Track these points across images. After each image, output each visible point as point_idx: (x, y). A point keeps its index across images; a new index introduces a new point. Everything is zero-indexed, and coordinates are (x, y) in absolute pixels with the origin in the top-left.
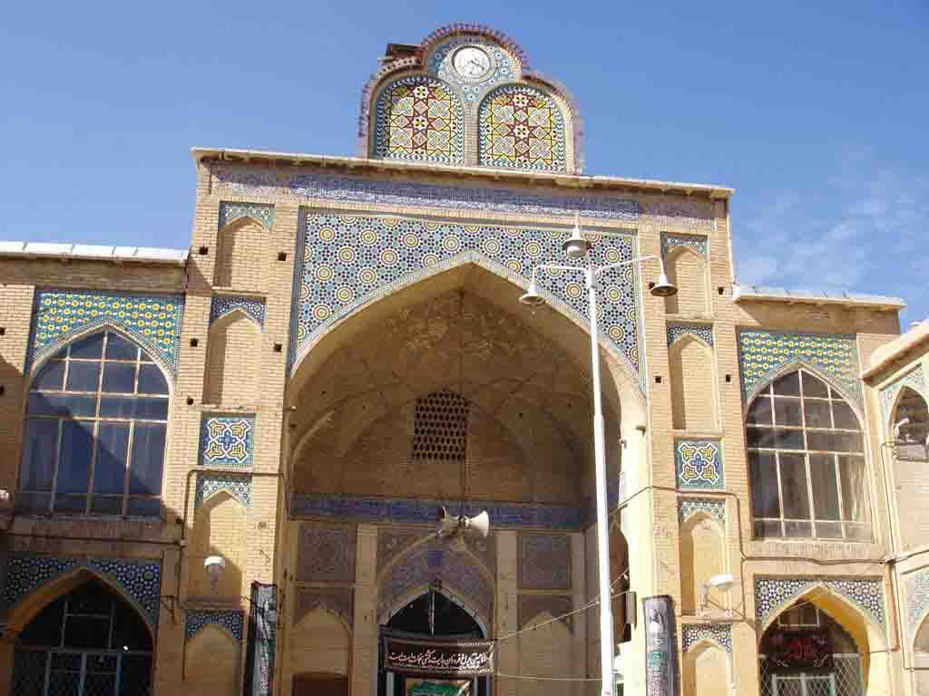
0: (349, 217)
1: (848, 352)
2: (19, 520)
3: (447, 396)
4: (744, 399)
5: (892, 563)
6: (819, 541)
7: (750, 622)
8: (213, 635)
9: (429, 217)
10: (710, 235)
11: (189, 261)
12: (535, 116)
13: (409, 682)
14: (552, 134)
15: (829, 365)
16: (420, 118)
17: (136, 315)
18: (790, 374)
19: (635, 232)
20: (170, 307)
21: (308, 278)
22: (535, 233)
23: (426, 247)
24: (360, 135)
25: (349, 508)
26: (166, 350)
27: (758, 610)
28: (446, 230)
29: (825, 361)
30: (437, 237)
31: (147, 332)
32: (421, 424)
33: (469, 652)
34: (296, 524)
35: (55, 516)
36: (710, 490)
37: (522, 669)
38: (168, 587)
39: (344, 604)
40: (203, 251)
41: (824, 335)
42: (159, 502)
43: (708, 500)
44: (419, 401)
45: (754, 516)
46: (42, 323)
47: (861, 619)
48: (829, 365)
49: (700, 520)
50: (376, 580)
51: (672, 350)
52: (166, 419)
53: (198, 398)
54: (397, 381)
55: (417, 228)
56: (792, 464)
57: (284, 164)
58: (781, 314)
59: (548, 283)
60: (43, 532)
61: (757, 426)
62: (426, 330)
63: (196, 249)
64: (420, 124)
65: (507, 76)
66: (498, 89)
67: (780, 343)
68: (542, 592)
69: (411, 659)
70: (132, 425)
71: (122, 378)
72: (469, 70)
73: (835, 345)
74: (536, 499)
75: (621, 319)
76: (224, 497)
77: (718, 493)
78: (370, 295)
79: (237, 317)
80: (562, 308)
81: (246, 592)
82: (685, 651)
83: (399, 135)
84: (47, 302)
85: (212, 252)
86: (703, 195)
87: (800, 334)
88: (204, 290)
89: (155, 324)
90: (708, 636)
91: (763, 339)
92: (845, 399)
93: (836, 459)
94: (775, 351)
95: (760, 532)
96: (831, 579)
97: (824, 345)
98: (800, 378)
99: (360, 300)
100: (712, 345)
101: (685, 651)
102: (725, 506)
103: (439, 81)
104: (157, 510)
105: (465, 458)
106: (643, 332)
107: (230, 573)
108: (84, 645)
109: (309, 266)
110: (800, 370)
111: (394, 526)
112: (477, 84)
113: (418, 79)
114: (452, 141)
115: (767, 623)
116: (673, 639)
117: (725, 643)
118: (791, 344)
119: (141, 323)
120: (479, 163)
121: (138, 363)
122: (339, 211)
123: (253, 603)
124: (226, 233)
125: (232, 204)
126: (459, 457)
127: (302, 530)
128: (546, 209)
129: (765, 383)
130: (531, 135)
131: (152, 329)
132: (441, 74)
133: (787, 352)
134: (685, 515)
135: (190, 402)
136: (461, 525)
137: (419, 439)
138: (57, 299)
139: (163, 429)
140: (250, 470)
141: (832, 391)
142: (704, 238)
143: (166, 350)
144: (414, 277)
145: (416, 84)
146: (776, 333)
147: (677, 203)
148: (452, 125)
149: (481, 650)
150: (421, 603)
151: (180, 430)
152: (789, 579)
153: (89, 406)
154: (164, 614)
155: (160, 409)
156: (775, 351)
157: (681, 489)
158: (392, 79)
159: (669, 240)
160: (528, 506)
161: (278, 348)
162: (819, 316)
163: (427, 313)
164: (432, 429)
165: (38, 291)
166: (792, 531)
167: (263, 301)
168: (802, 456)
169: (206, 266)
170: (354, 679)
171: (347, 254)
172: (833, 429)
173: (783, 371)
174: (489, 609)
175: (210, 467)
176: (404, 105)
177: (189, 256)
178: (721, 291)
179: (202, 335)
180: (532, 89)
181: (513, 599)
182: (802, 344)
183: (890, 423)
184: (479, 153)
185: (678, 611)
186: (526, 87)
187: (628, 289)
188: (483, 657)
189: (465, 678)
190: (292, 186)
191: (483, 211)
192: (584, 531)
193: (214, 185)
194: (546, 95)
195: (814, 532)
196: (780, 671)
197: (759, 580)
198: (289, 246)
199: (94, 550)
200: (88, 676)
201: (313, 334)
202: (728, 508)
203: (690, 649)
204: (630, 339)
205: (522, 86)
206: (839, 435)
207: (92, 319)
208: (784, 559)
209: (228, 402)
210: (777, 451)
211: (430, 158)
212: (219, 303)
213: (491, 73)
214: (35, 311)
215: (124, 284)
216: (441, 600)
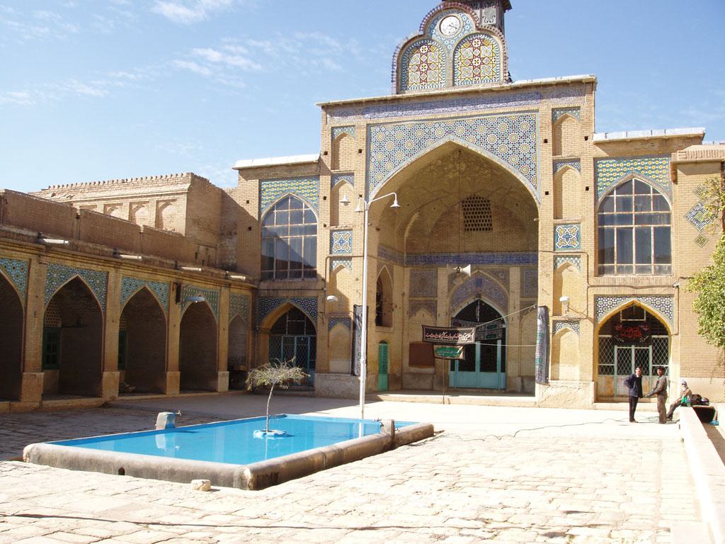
0: (390, 126)
1: (665, 165)
2: (262, 283)
4: (596, 200)
6: (637, 276)
7: (590, 319)
8: (340, 328)
9: (428, 120)
10: (582, 106)
11: (320, 160)
12: (485, 51)
13: (435, 347)
14: (493, 60)
16: (424, 65)
17: (300, 188)
18: (626, 183)
19: (537, 111)
20: (314, 182)
21: (373, 160)
22: (482, 119)
24: (392, 81)
27: (596, 313)
28: (437, 125)
29: (650, 172)
30: (432, 130)
33: (463, 333)
35: (276, 281)
36: (572, 251)
37: (523, 339)
38: (320, 309)
41: (650, 156)
42: (316, 271)
43: (572, 256)
45: (599, 263)
49: (568, 266)
50: (448, 297)
51: (557, 175)
52: (316, 234)
53: (328, 224)
54: (446, 194)
55: (422, 126)
56: (624, 234)
57: (359, 103)
58: (622, 148)
59: (489, 147)
60: (271, 288)
61: (605, 213)
62: (455, 168)
63: (322, 153)
64: (424, 68)
65: (468, 30)
66: (464, 39)
67: (622, 165)
69: (436, 336)
70: (303, 238)
71: (297, 217)
72: (448, 31)
73: (657, 162)
74: (530, 249)
75: (528, 162)
76: (341, 267)
77: (576, 252)
78: (401, 165)
79: (343, 183)
80: (496, 160)
81: (351, 309)
82: (554, 333)
83: (413, 76)
84: (264, 186)
85: (330, 154)
86: (579, 82)
87: (634, 158)
88: (327, 172)
90: (568, 326)
91: (612, 163)
92: (661, 194)
93: (652, 229)
94: (618, 170)
95: (600, 272)
96: (641, 296)
97: (650, 163)
98: (633, 184)
99: (397, 168)
100: (579, 170)
101: (554, 333)
103: (433, 41)
104: (313, 274)
107: (343, 300)
108: (297, 333)
109: (373, 154)
110: (633, 180)
115: (603, 318)
116: (547, 328)
117: (577, 330)
118: (628, 164)
119: (303, 191)
120: (454, 85)
121: (304, 209)
122: (385, 123)
123: (355, 314)
124: (335, 144)
125: (337, 128)
127: (413, 275)
128: (489, 106)
129: (610, 190)
131: (308, 193)
132: (434, 37)
134: (558, 264)
135: (325, 226)
136: (459, 272)
139: (315, 238)
140: (351, 255)
141: (654, 190)
142: (579, 108)
144: (423, 152)
145: (421, 45)
146: (619, 159)
147: (564, 89)
148: (440, 66)
149: (468, 332)
151: (322, 237)
152: (616, 296)
153: (285, 231)
154: (319, 320)
155: (314, 230)
157: (556, 251)
158: (409, 45)
159: (558, 112)
162: (647, 146)
163: (452, 160)
165: (260, 180)
166: (620, 270)
167: (353, 174)
168: (632, 228)
169: (327, 161)
171: (390, 146)
172: (652, 212)
173: (621, 181)
174: (506, 309)
175: (335, 255)
176: (416, 59)
177: (320, 157)
178: (586, 138)
180: (483, 34)
181: (518, 303)
182: (636, 164)
184: (454, 79)
185: (550, 313)
186: (480, 34)
187: (532, 145)
188: (469, 335)
189: (461, 345)
190: (363, 114)
191: (455, 112)
193: (328, 119)
194: (491, 37)
195: (634, 270)
196: (620, 344)
197: (597, 298)
198: (363, 146)
199: (291, 294)
200: (297, 346)
202: (583, 260)
203: (557, 332)
204: (533, 172)
205: (477, 34)
206: (655, 215)
207: (283, 192)
208: (612, 286)
209: (342, 224)
210: (616, 227)
212: (334, 177)
213: (461, 29)
214: (260, 191)
215: (294, 174)
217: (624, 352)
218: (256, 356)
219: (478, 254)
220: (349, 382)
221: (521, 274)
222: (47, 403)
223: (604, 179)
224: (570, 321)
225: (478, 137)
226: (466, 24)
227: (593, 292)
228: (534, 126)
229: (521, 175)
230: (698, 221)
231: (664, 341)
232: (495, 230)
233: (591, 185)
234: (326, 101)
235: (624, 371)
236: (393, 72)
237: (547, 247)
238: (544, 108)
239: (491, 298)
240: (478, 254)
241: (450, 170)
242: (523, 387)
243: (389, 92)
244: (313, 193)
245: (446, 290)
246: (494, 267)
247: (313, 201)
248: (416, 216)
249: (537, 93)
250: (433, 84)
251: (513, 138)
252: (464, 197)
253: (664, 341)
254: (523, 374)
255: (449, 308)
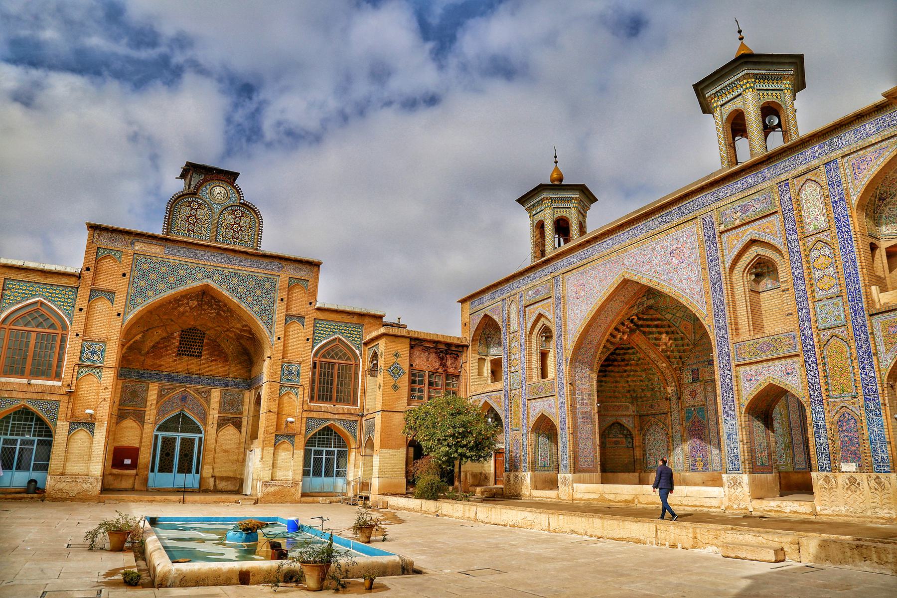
1: (359, 332)
3: (195, 330)
5: (362, 416)
15: (350, 337)
17: (54, 295)
20: (70, 293)
23: (188, 276)
25: (144, 377)
26: (67, 312)
28: (198, 269)
29: (349, 335)
31: (59, 303)
32: (183, 341)
34: (121, 382)
39: (140, 418)
40: (88, 269)
44: (183, 331)
46: (7, 295)
47: (347, 437)
48: (350, 337)
50: (156, 408)
53: (81, 334)
54: (173, 323)
55: (185, 267)
62: (188, 303)
63: (85, 269)
65: (233, 202)
68: (231, 416)
75: (267, 313)
77: (297, 385)
78: (161, 295)
80: (243, 306)
89: (63, 300)
94: (329, 330)
100: (303, 326)
102: (299, 390)
105: (201, 357)
106: (276, 318)
111: (168, 384)
112: (220, 204)
113: (194, 199)
114: (205, 230)
120: (216, 241)
126: (199, 356)
130: (241, 230)
133: (334, 330)
135: (77, 335)
137: (181, 347)
138: (15, 285)
143: (67, 312)
150: (178, 416)
156: (329, 330)
160: (227, 379)
161: (119, 315)
164: (191, 340)
170: (142, 449)
176: (185, 211)
178: (311, 304)
179: (85, 306)
183: (370, 363)
187: (272, 300)
192: (250, 391)
201: (135, 310)
202: (300, 391)
204: (270, 321)
211: (195, 236)
216: (185, 416)
217: (318, 459)
218: (635, 458)
219: (187, 375)
220: (86, 484)
221: (221, 395)
222: (303, 498)
223: (320, 335)
224: (287, 436)
225: (231, 286)
226: (232, 197)
227: (305, 415)
228: (274, 287)
229: (260, 321)
230: (394, 374)
231: (345, 452)
232: (204, 357)
233: (311, 337)
234: (94, 222)
235: (317, 474)
236: (166, 216)
237: (275, 378)
238: (283, 276)
239: (193, 413)
240: (187, 375)
241: (183, 304)
242: (215, 485)
243: (159, 231)
244: (68, 303)
245: (155, 402)
246: (200, 387)
247: (67, 310)
248: (138, 337)
249: (280, 263)
250: (198, 235)
251: (258, 292)
252: (185, 327)
253: (345, 452)
254: (217, 474)
255: (156, 418)
